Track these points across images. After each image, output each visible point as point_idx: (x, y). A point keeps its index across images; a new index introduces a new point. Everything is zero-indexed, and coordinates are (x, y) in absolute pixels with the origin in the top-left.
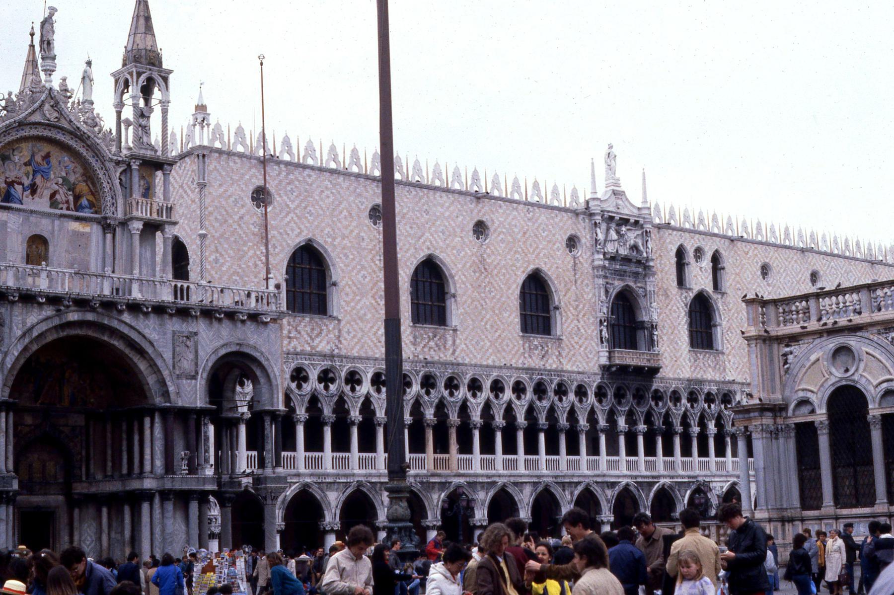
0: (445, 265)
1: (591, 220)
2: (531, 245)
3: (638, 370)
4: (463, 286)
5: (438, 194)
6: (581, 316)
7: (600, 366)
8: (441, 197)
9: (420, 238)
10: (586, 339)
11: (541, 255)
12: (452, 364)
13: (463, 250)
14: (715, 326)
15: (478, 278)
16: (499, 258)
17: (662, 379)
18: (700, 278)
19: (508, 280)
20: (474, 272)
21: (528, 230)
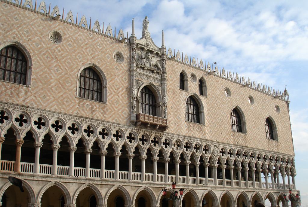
0: (26, 50)
1: (130, 47)
2: (90, 51)
3: (154, 126)
4: (37, 63)
5: (27, 12)
6: (120, 94)
7: (130, 122)
8: (29, 14)
9: (8, 31)
10: (122, 106)
11: (97, 58)
12: (23, 106)
13: (41, 44)
14: (201, 112)
15: (50, 61)
16: (67, 53)
17: (168, 133)
18: (193, 88)
19: (71, 67)
20: (48, 57)
21: (89, 43)
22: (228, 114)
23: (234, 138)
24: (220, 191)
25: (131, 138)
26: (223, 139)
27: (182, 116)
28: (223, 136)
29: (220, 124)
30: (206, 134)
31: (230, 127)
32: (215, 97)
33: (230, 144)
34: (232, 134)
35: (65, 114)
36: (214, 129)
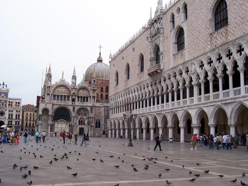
17: (163, 73)
22: (205, 19)
23: (211, 42)
24: (195, 109)
25: (152, 85)
26: (200, 52)
27: (171, 53)
28: (199, 49)
29: (197, 37)
30: (186, 56)
31: (207, 31)
32: (194, 11)
33: (206, 53)
34: (209, 39)
35: (135, 85)
36: (192, 47)
